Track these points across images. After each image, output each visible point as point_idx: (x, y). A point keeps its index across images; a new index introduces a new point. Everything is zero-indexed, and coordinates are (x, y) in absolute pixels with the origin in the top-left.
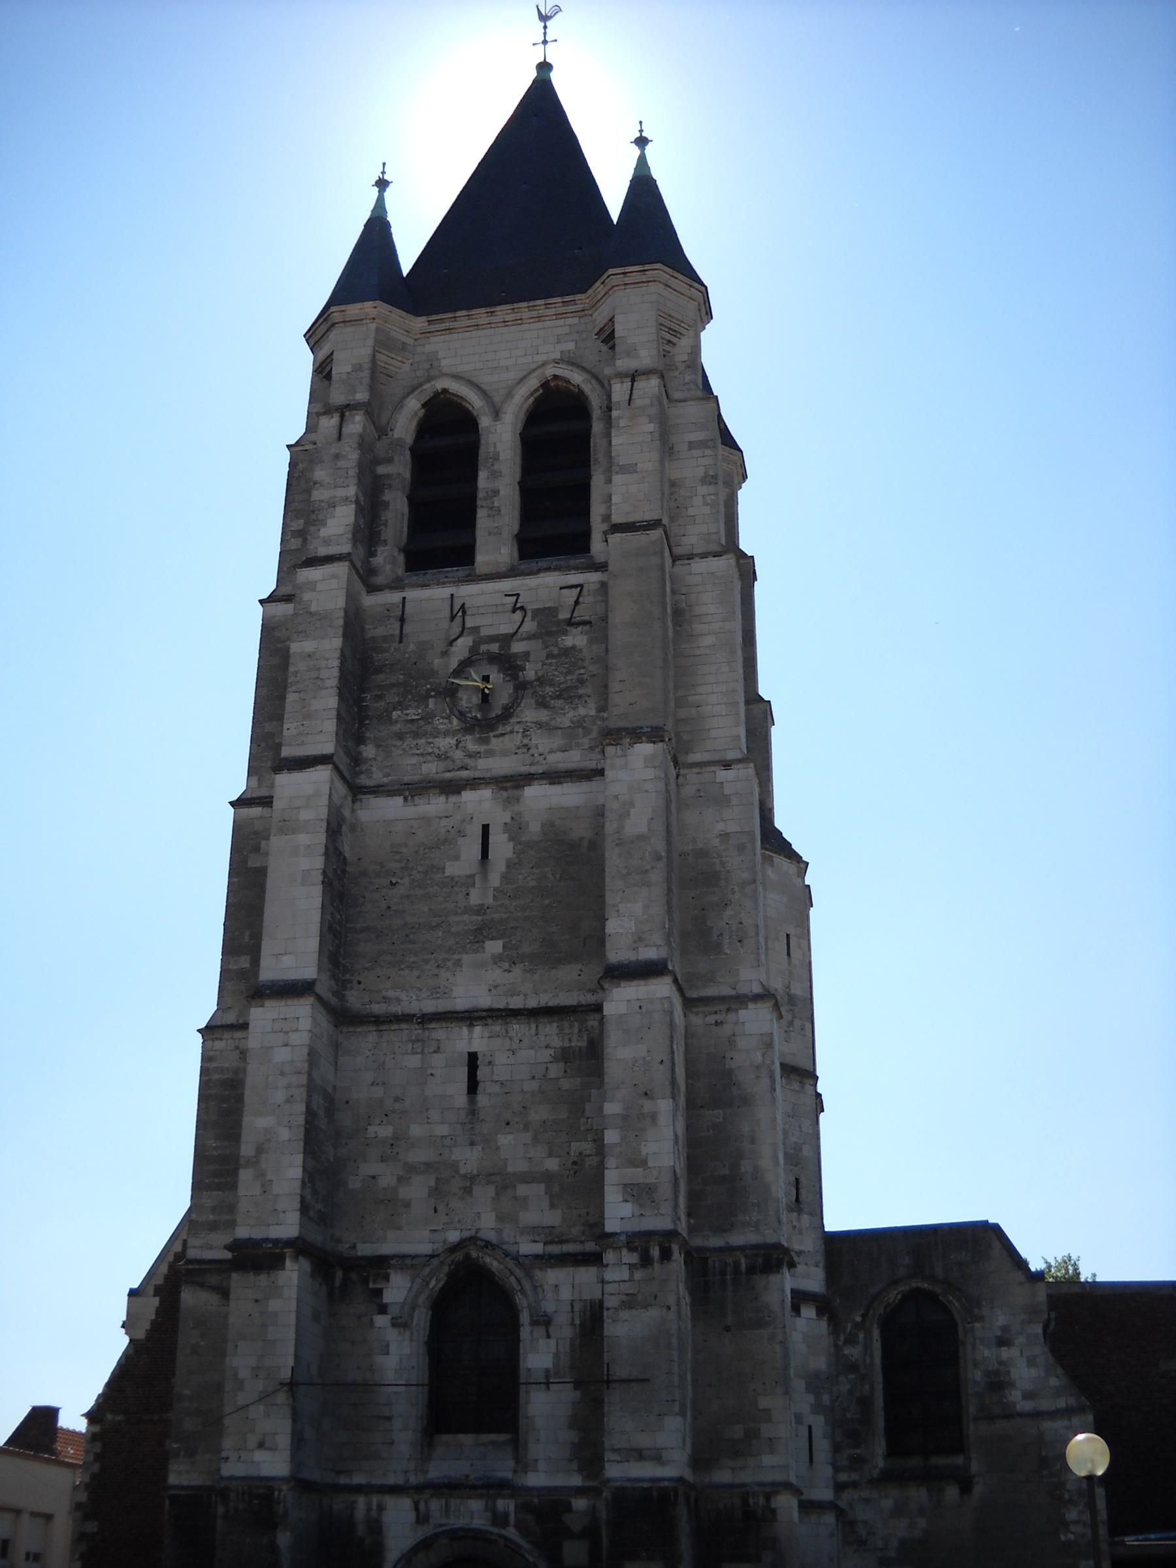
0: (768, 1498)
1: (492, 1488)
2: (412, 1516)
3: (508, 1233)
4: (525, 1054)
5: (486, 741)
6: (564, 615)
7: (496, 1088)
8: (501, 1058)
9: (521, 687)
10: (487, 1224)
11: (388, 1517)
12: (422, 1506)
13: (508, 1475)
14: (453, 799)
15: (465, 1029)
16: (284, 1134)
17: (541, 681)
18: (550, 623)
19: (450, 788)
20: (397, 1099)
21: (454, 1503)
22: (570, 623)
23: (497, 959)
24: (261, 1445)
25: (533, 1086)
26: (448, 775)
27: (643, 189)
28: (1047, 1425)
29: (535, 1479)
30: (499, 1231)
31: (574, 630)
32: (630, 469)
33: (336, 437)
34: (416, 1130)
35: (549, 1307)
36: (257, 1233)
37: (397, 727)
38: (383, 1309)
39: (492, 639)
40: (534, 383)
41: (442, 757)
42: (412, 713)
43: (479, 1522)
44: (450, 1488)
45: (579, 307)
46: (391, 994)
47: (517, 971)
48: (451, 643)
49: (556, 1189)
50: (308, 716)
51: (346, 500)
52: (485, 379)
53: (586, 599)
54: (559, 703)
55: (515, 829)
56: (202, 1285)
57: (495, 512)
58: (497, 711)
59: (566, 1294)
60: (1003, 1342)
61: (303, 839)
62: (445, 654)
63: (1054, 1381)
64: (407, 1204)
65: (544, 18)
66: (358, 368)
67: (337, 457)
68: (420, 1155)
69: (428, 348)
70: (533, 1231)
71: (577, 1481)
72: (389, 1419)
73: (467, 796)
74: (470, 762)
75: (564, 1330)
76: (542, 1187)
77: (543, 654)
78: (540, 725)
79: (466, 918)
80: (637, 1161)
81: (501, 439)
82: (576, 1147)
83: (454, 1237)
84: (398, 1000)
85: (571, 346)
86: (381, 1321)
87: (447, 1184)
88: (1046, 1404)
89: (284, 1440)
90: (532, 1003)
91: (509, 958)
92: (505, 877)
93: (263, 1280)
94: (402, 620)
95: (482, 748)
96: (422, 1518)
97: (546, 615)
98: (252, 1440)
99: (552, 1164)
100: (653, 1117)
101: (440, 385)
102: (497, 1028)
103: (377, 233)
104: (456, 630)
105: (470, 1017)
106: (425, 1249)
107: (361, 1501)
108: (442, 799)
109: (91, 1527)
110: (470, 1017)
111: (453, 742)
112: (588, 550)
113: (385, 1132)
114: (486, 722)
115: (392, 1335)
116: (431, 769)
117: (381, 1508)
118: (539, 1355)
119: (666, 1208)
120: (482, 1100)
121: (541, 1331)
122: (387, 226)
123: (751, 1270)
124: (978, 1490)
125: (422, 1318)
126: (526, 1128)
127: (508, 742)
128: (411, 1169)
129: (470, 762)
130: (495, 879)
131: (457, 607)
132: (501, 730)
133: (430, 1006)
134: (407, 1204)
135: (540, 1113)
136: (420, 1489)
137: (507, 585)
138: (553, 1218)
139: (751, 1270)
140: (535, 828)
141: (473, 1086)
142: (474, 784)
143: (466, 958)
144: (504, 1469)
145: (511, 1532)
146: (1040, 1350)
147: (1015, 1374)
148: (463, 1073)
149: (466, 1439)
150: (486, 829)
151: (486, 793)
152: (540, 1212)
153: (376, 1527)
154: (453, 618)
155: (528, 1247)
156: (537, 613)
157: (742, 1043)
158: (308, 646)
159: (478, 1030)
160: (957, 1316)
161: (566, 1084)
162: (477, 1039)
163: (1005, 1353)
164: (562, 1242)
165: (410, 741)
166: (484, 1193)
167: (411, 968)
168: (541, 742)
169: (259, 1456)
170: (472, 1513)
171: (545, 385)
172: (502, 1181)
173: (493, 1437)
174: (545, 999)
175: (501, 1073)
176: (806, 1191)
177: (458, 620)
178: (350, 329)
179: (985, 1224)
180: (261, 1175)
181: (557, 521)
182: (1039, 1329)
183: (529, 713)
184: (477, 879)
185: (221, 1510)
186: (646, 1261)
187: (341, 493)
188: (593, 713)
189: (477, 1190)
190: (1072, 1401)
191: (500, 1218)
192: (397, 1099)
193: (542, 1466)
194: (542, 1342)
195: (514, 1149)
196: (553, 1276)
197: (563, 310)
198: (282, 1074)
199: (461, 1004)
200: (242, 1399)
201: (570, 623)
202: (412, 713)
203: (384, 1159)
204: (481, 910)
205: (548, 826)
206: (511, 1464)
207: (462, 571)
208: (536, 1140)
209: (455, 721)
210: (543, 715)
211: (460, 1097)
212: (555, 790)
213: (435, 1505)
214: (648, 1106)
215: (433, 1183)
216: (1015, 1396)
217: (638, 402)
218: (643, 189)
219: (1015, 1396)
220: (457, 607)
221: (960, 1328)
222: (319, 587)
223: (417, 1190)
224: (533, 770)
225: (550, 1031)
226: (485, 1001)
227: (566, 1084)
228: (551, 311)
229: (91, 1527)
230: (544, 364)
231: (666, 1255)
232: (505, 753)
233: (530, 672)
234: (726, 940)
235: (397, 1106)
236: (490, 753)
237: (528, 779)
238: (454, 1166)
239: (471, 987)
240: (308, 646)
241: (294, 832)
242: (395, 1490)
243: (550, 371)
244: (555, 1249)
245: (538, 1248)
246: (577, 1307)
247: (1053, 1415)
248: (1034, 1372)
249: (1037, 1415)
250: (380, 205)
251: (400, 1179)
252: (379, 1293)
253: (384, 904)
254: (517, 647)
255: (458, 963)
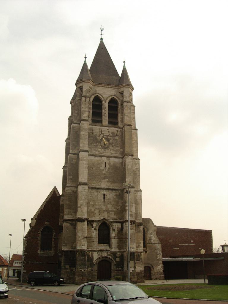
0: (141, 253)
1: (107, 251)
2: (97, 254)
3: (109, 218)
4: (111, 195)
5: (105, 150)
6: (115, 134)
7: (107, 199)
8: (108, 195)
9: (110, 143)
10: (106, 217)
11: (94, 254)
12: (98, 253)
13: (109, 249)
14: (101, 158)
15: (103, 191)
16: (85, 204)
17: (112, 143)
18: (113, 135)
19: (101, 156)
20: (94, 199)
21: (103, 253)
22: (116, 135)
23: (107, 181)
24: (83, 245)
25: (112, 199)
26: (100, 154)
27: (124, 71)
28: (156, 245)
29: (113, 250)
30: (108, 218)
31: (117, 137)
32: (127, 116)
33: (85, 101)
34: (97, 203)
35: (114, 228)
36: (81, 217)
37: (93, 146)
38: (93, 227)
39: (105, 136)
40: (110, 98)
41: (99, 152)
42: (95, 144)
43: (106, 255)
44: (102, 251)
45: (117, 87)
46: (93, 184)
47: (110, 183)
48: (100, 135)
49: (115, 213)
50: (84, 144)
51: (87, 111)
52: (103, 95)
53: (118, 132)
54: (115, 147)
55: (109, 163)
56: (67, 222)
57: (105, 116)
58: (106, 146)
59: (116, 226)
60: (151, 234)
61: (85, 162)
62: (99, 137)
63: (157, 239)
64: (96, 213)
65: (102, 30)
66: (87, 90)
67: (85, 104)
68: (97, 207)
69: (95, 88)
70: (112, 218)
71: (118, 250)
72: (94, 242)
73: (102, 158)
74: (103, 153)
75: (116, 231)
76: (113, 212)
77: (113, 139)
78: (112, 149)
79: (103, 175)
80: (131, 212)
81: (106, 105)
82: (118, 208)
83: (102, 218)
84: (94, 185)
85: (116, 93)
86: (93, 229)
87: (101, 211)
88: (156, 242)
89: (86, 245)
90: (112, 188)
91: (109, 181)
92: (108, 170)
93: (82, 223)
94: (93, 130)
95: (105, 151)
96: (98, 255)
97: (113, 133)
98: (81, 244)
99: (115, 210)
100: (133, 206)
101: (97, 95)
102: (107, 191)
103: (85, 65)
104: (100, 133)
105: (104, 189)
106: (98, 219)
107: (90, 252)
108: (99, 158)
109: (26, 253)
110: (104, 189)
111: (100, 150)
112: (117, 125)
113: (93, 203)
114: (105, 148)
115: (94, 231)
116: (97, 153)
117: (93, 253)
118: (113, 234)
119: (134, 218)
120: (105, 200)
121: (113, 231)
122: (86, 64)
123: (139, 225)
124: (147, 252)
125: (97, 229)
126: (111, 205)
127: (109, 151)
128: (96, 209)
129: (103, 153)
130: (107, 170)
131: (101, 130)
132: (107, 149)
133: (98, 187)
134: (96, 213)
135: (113, 203)
136: (98, 251)
137: (108, 128)
138: (115, 217)
139: (139, 225)
140: (112, 164)
141: (104, 198)
142: (104, 156)
143: (103, 181)
144: (108, 248)
145: (110, 257)
146: (155, 235)
147: (152, 238)
148: (103, 196)
149: (102, 244)
150: (105, 163)
151: (106, 158)
152: (113, 216)
153: (92, 256)
154: (100, 131)
155: (112, 220)
156: (112, 133)
157: (138, 196)
158: (83, 133)
159: (105, 191)
160: (145, 230)
161: (116, 199)
162: (105, 192)
163: (151, 235)
164: (116, 220)
165: (94, 149)
166: (106, 213)
167: (96, 181)
168: (113, 152)
169: (82, 247)
170: (105, 254)
171: (112, 98)
172: (108, 211)
173: (105, 244)
174: (113, 188)
175: (108, 197)
176: (141, 216)
177: (101, 132)
178: (85, 83)
179: (149, 219)
180: (81, 209)
181: (113, 120)
182: (155, 233)
183: (111, 148)
184: (104, 170)
185: (77, 254)
186: (132, 224)
187: (87, 110)
188: (119, 149)
189: (105, 212)
190: (159, 242)
191: (108, 216)
192: (94, 199)
193: (114, 248)
194: (114, 233)
195: (110, 207)
196: (114, 224)
197: (115, 87)
198: (84, 195)
199: (102, 187)
200: (80, 239)
201: (116, 135)
202: (95, 144)
203: (92, 207)
204: (105, 174)
205: (114, 164)
206: (109, 248)
207: (100, 124)
208: (112, 206)
209: (101, 147)
210: (113, 148)
211: (103, 200)
212: (115, 159)
213: (100, 253)
214: (132, 204)
215: (99, 211)
216: (152, 241)
217: (128, 106)
218: (124, 71)
219: (152, 241)
220: (101, 130)
221: (146, 232)
222: (85, 124)
223: (97, 211)
224: (112, 155)
225: (114, 192)
226: (106, 187)
227: (116, 199)
228: (113, 87)
229: (26, 253)
230: (112, 95)
231: (134, 223)
232: (108, 152)
233: (111, 141)
234: (136, 183)
235: (94, 200)
236: (105, 152)
237: (111, 157)
238: (102, 209)
239: (104, 185)
240: (83, 133)
241: (83, 161)
242: (95, 251)
243: (113, 97)
244: (115, 221)
245: (113, 220)
246: (118, 228)
247: (157, 244)
248: (155, 238)
249: (155, 243)
250: (85, 61)
251: (95, 210)
252: (92, 225)
253: (91, 172)
254: (109, 138)
255: (102, 181)
